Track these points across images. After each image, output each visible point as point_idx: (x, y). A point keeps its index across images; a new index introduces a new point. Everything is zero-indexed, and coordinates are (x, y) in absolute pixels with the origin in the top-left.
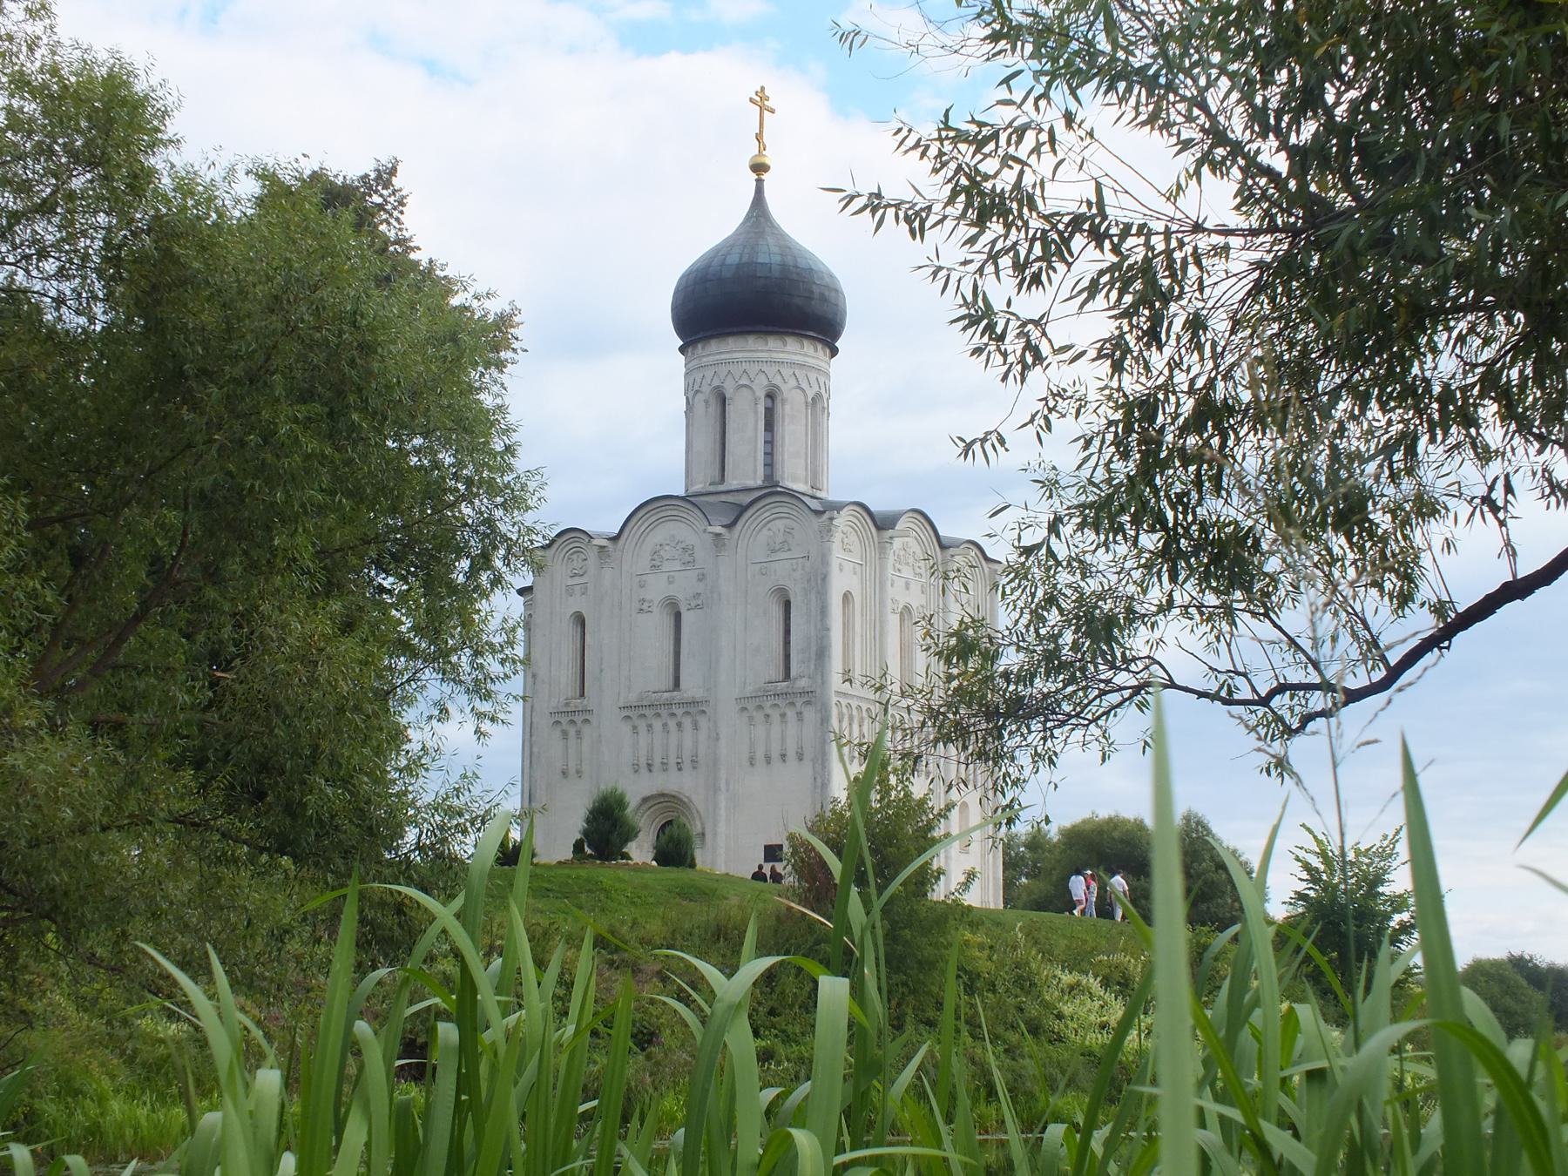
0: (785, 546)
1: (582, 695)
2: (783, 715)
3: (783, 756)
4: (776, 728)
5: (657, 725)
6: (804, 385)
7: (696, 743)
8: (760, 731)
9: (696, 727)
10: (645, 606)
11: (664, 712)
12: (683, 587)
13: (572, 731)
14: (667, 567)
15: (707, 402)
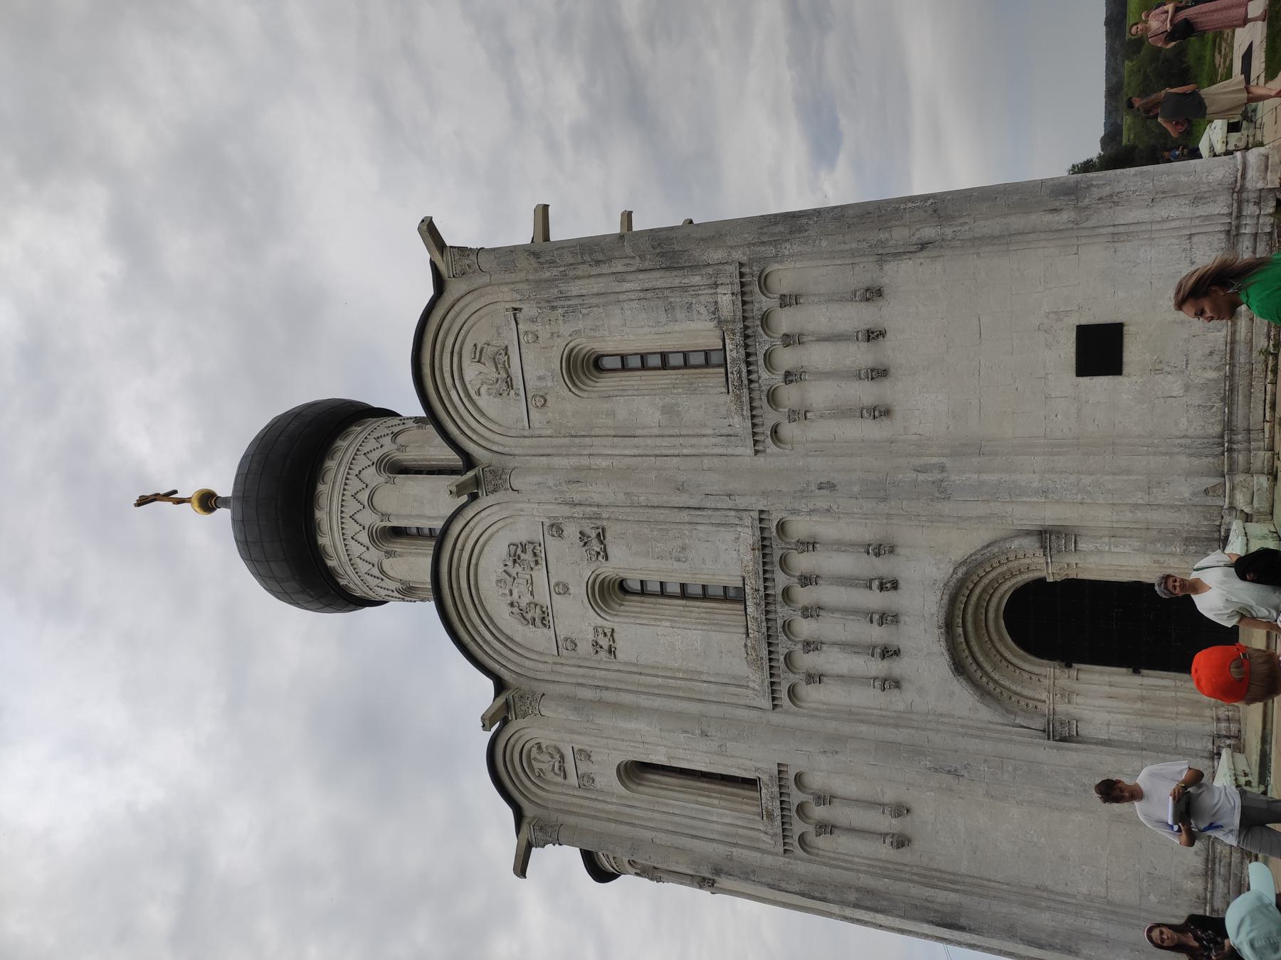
0: (500, 359)
1: (751, 783)
2: (789, 340)
3: (873, 335)
4: (816, 356)
5: (805, 628)
6: (396, 429)
7: (841, 546)
8: (819, 394)
9: (809, 545)
10: (604, 642)
11: (782, 612)
12: (571, 566)
13: (819, 812)
14: (542, 596)
15: (389, 554)
